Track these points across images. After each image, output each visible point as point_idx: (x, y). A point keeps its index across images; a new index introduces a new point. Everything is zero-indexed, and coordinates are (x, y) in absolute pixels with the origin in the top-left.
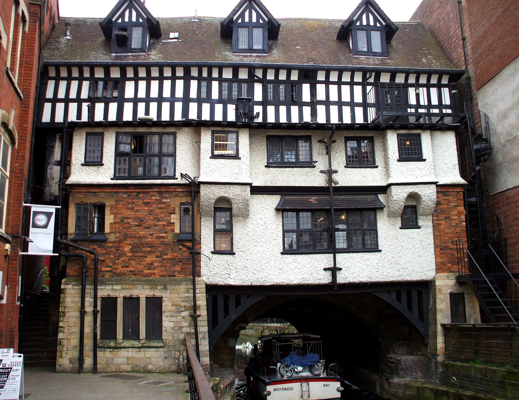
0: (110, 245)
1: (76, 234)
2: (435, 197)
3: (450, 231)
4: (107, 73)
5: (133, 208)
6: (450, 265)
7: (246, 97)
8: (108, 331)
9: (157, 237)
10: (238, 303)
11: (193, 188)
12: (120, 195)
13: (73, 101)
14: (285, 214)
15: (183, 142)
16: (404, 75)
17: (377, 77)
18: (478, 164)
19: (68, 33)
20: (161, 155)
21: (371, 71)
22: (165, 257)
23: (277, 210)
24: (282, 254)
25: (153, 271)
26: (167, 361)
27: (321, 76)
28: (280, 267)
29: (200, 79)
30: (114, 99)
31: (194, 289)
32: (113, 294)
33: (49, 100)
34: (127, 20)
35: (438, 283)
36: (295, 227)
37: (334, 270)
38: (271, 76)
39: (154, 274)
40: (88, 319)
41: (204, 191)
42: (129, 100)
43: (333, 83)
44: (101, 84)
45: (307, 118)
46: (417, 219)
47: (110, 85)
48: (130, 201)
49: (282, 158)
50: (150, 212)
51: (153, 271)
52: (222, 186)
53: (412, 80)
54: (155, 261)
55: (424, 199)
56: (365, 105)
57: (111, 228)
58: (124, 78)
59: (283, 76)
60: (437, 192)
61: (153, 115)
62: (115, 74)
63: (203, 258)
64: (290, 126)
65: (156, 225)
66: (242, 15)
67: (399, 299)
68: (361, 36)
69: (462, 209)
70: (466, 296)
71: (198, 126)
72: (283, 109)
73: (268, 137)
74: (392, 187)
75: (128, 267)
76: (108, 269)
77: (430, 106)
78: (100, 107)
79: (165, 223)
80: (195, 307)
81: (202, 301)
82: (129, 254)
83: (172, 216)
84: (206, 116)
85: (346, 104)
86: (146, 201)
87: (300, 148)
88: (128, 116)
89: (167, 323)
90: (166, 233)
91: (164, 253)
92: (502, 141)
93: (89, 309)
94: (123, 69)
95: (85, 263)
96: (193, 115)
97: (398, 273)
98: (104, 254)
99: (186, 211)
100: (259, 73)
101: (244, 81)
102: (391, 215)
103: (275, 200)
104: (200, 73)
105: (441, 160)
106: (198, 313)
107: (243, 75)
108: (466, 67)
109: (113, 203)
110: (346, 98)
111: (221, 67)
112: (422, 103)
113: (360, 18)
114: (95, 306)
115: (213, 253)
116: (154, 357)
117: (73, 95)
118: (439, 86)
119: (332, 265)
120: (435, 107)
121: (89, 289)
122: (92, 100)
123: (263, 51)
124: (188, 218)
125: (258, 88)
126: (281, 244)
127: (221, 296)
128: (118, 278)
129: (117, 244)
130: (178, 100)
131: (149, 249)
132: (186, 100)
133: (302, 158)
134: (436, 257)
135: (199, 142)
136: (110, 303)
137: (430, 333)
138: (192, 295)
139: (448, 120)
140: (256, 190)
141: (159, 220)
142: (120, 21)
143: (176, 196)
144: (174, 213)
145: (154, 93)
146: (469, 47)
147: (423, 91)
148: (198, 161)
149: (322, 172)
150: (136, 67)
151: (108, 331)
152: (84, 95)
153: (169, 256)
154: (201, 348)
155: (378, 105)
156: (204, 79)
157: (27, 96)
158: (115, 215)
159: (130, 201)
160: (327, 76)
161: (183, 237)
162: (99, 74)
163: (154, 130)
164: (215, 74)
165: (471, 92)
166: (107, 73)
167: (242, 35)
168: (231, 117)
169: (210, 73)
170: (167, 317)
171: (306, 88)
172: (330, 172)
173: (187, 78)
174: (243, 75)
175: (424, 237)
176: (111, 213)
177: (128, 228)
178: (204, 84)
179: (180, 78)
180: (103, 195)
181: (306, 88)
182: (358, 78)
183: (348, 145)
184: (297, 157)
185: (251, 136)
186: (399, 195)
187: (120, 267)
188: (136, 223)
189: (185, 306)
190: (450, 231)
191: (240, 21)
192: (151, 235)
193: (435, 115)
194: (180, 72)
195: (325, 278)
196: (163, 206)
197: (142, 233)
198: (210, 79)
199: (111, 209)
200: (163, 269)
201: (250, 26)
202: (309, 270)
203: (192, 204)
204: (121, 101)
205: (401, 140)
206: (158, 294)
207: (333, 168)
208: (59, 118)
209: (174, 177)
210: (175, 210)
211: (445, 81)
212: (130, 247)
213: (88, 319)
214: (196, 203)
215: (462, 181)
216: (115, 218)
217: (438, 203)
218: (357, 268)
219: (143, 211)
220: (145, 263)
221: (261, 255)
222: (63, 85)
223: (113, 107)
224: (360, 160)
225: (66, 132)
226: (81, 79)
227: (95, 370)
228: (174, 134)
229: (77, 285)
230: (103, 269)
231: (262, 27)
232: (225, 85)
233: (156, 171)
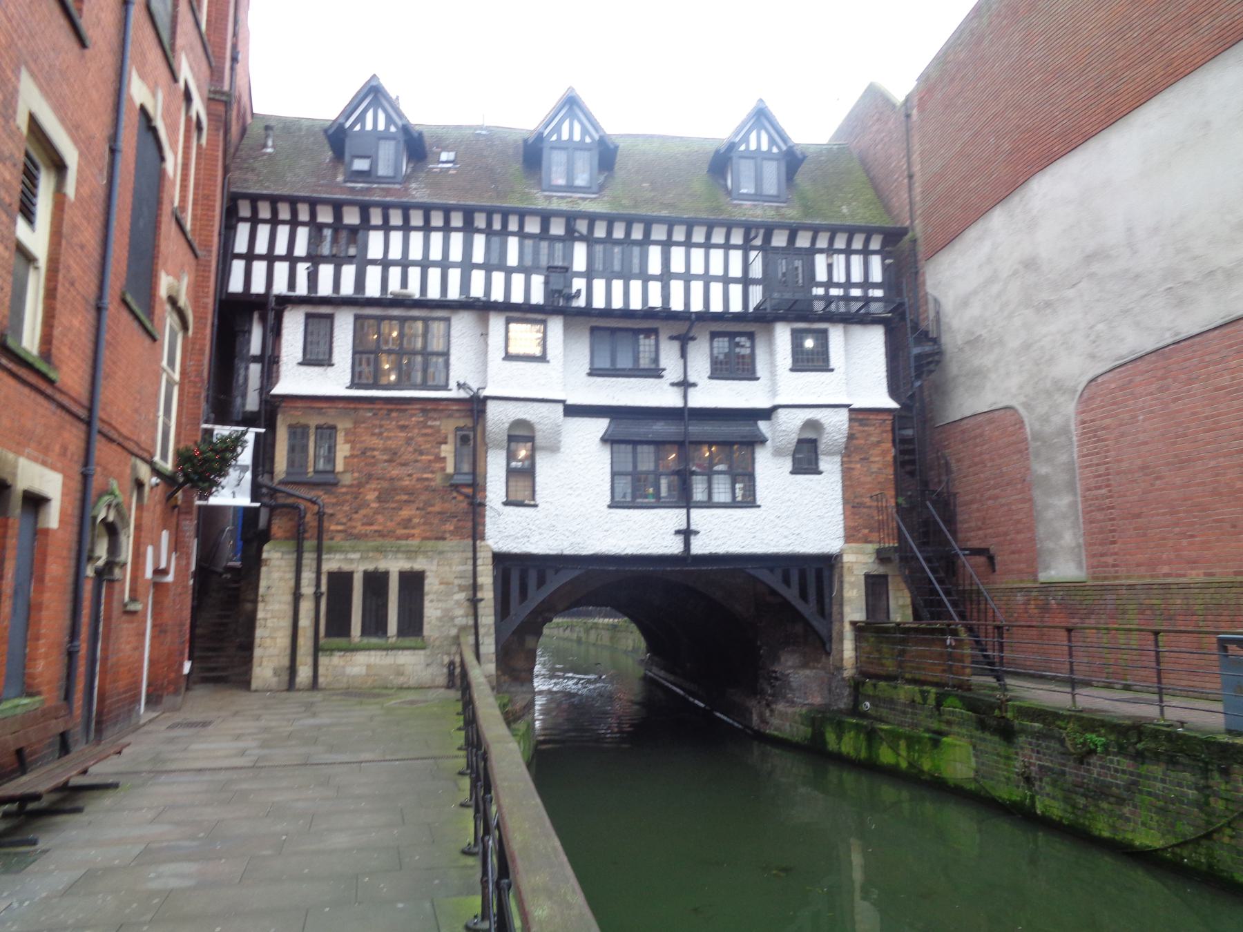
0: (344, 490)
1: (288, 473)
2: (846, 426)
3: (869, 479)
4: (338, 216)
5: (381, 434)
6: (866, 531)
7: (560, 264)
8: (337, 623)
9: (418, 480)
10: (541, 582)
11: (475, 406)
12: (361, 413)
13: (281, 258)
14: (616, 446)
16: (809, 234)
17: (767, 238)
18: (918, 377)
19: (270, 143)
20: (426, 354)
21: (758, 226)
22: (430, 509)
23: (604, 440)
24: (610, 507)
25: (412, 531)
26: (430, 670)
28: (607, 527)
29: (489, 231)
30: (350, 260)
31: (475, 559)
32: (346, 567)
33: (239, 256)
34: (369, 126)
35: (847, 558)
36: (630, 468)
37: (687, 534)
38: (600, 232)
39: (413, 536)
40: (306, 607)
41: (492, 409)
42: (374, 262)
43: (698, 245)
44: (328, 233)
45: (655, 301)
46: (817, 460)
47: (344, 235)
48: (377, 422)
49: (613, 360)
50: (409, 441)
51: (412, 531)
52: (520, 404)
53: (822, 243)
54: (415, 516)
55: (828, 429)
56: (746, 281)
57: (346, 464)
58: (365, 225)
59: (619, 233)
60: (851, 420)
61: (414, 290)
62: (351, 217)
63: (489, 513)
64: (626, 313)
65: (417, 461)
66: (558, 129)
67: (786, 581)
68: (746, 170)
69: (889, 445)
70: (890, 579)
71: (483, 308)
72: (618, 285)
73: (593, 330)
74: (780, 410)
75: (371, 524)
76: (340, 528)
77: (848, 284)
78: (326, 271)
79: (431, 458)
80: (475, 587)
81: (486, 577)
82: (374, 505)
83: (443, 447)
84: (497, 295)
85: (716, 279)
86: (401, 423)
87: (642, 348)
88: (373, 289)
89: (432, 611)
90: (432, 472)
91: (428, 503)
92: (960, 342)
93: (307, 589)
94: (364, 209)
95: (301, 517)
96: (477, 291)
97: (784, 541)
98: (334, 505)
99: (464, 440)
100: (582, 226)
101: (557, 238)
102: (778, 453)
103: (602, 425)
104: (489, 223)
105: (859, 372)
106: (479, 595)
107: (557, 229)
108: (912, 222)
109: (349, 425)
111: (522, 215)
112: (835, 280)
113: (745, 139)
114: (318, 585)
115: (506, 504)
116: (411, 664)
117: (281, 249)
118: (866, 252)
119: (684, 526)
120: (856, 285)
121: (309, 558)
122: (314, 259)
124: (467, 450)
125: (580, 250)
126: (609, 493)
127: (515, 570)
129: (355, 489)
130: (455, 265)
131: (405, 497)
132: (467, 266)
133: (644, 363)
134: (845, 518)
135: (485, 335)
136: (341, 582)
137: (834, 634)
138: (471, 568)
139: (875, 308)
140: (573, 411)
141: (421, 453)
142: (358, 128)
143: (450, 416)
144: (446, 443)
145: (416, 253)
146: (918, 189)
147: (839, 260)
148: (485, 363)
149: (673, 384)
150: (386, 208)
151: (337, 623)
152: (301, 249)
153: (437, 508)
154: (483, 650)
155: (765, 281)
156: (496, 233)
157: (207, 248)
158: (352, 442)
159: (377, 422)
160: (689, 235)
161: (459, 479)
162: (325, 216)
163: (415, 313)
164: (513, 226)
165: (916, 262)
166: (338, 216)
168: (538, 297)
169: (505, 224)
170: (432, 601)
172: (685, 385)
174: (557, 229)
176: (346, 442)
177: (374, 464)
178: (496, 240)
179: (457, 230)
180: (332, 412)
182: (737, 238)
183: (715, 344)
184: (636, 359)
185: (567, 328)
186: (789, 424)
187: (359, 524)
188: (385, 457)
189: (459, 586)
190: (869, 479)
191: (554, 138)
192: (410, 475)
193: (856, 299)
194: (457, 220)
195: (674, 546)
196: (428, 431)
197: (395, 472)
198: (504, 232)
199: (346, 434)
200: (427, 527)
201: (570, 147)
202: (649, 533)
203: (474, 429)
204: (363, 263)
205: (797, 337)
206: (418, 565)
207: (691, 379)
208: (258, 287)
209: (445, 387)
210: (446, 438)
211: (875, 244)
212: (376, 493)
213: (306, 607)
214: (479, 429)
215: (893, 405)
216: (352, 448)
217: (851, 437)
218: (723, 532)
219: (397, 439)
220: (398, 519)
221: (575, 508)
222: (263, 231)
223: (349, 272)
224: (735, 367)
225: (270, 309)
226: (294, 223)
227: (314, 685)
228: (448, 320)
229: (289, 553)
230: (333, 528)
231: (590, 150)
232: (529, 243)
233: (418, 378)
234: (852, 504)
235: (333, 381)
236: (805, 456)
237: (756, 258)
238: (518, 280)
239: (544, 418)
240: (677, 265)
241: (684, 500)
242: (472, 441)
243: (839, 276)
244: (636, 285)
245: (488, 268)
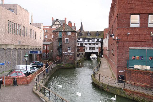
11: (84, 47)
15: (84, 44)
105: (99, 45)
136: (80, 53)
173: (84, 38)
175: (98, 50)
218: (94, 51)
221: (88, 50)
235: (79, 46)
236: (97, 48)
241: (92, 50)
242: (84, 48)
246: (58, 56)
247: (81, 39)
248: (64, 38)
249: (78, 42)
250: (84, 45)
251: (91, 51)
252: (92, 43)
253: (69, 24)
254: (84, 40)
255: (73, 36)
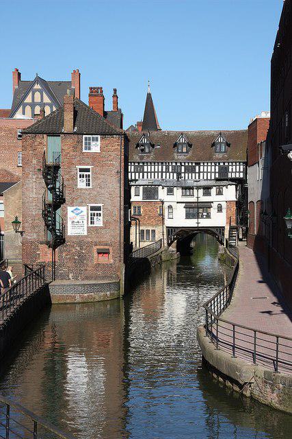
11: (163, 202)
17: (219, 164)
27: (202, 164)
37: (198, 223)
38: (187, 164)
40: (138, 235)
53: (230, 164)
72: (190, 174)
81: (165, 231)
93: (138, 232)
94: (143, 163)
100: (183, 164)
103: (184, 204)
105: (230, 193)
107: (179, 164)
110: (209, 170)
121: (138, 227)
123: (186, 153)
125: (183, 168)
127: (170, 230)
128: (145, 225)
150: (147, 163)
152: (132, 171)
167: (180, 147)
171: (197, 167)
181: (197, 167)
182: (213, 164)
201: (182, 144)
204: (143, 172)
213: (138, 235)
218: (204, 223)
221: (179, 219)
223: (141, 174)
234: (227, 218)
235: (140, 198)
237: (217, 167)
238: (171, 174)
239: (174, 205)
240: (202, 170)
243: (234, 170)
244: (193, 174)
245: (166, 172)
246: (44, 248)
247: (145, 167)
248: (71, 164)
249: (136, 180)
250: (162, 194)
251: (192, 223)
252: (199, 184)
253: (94, 99)
254: (162, 172)
255: (113, 154)
